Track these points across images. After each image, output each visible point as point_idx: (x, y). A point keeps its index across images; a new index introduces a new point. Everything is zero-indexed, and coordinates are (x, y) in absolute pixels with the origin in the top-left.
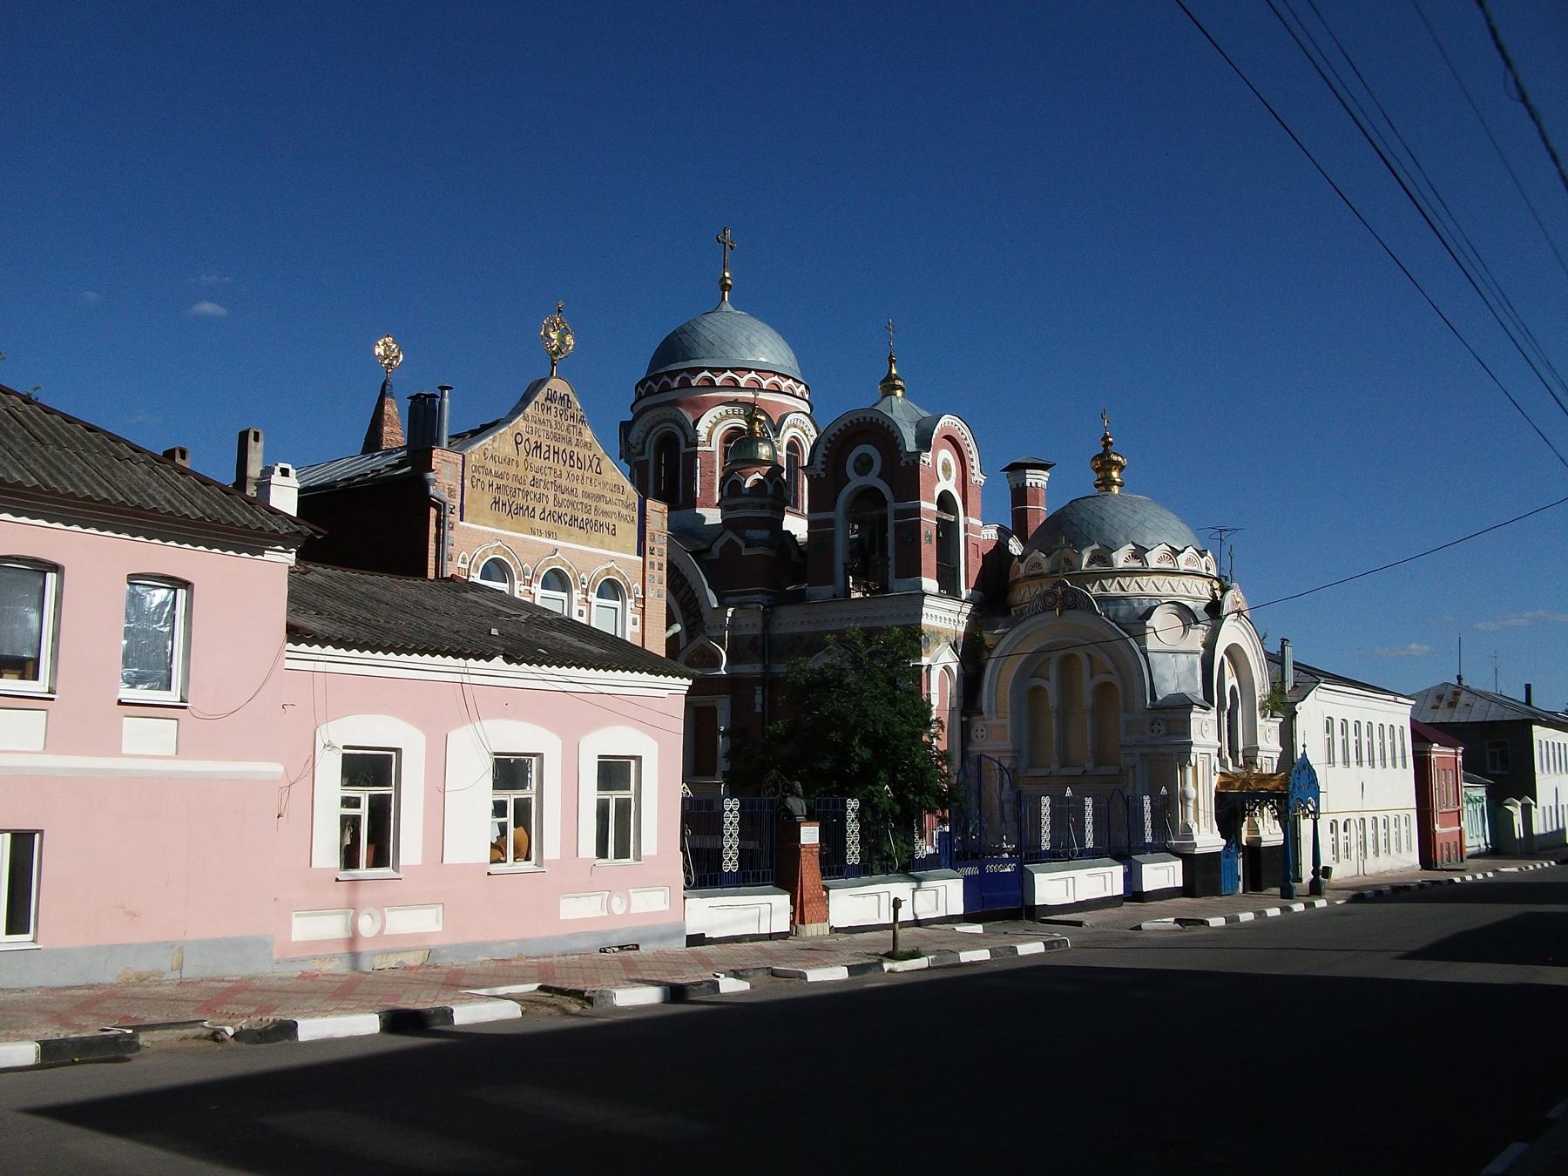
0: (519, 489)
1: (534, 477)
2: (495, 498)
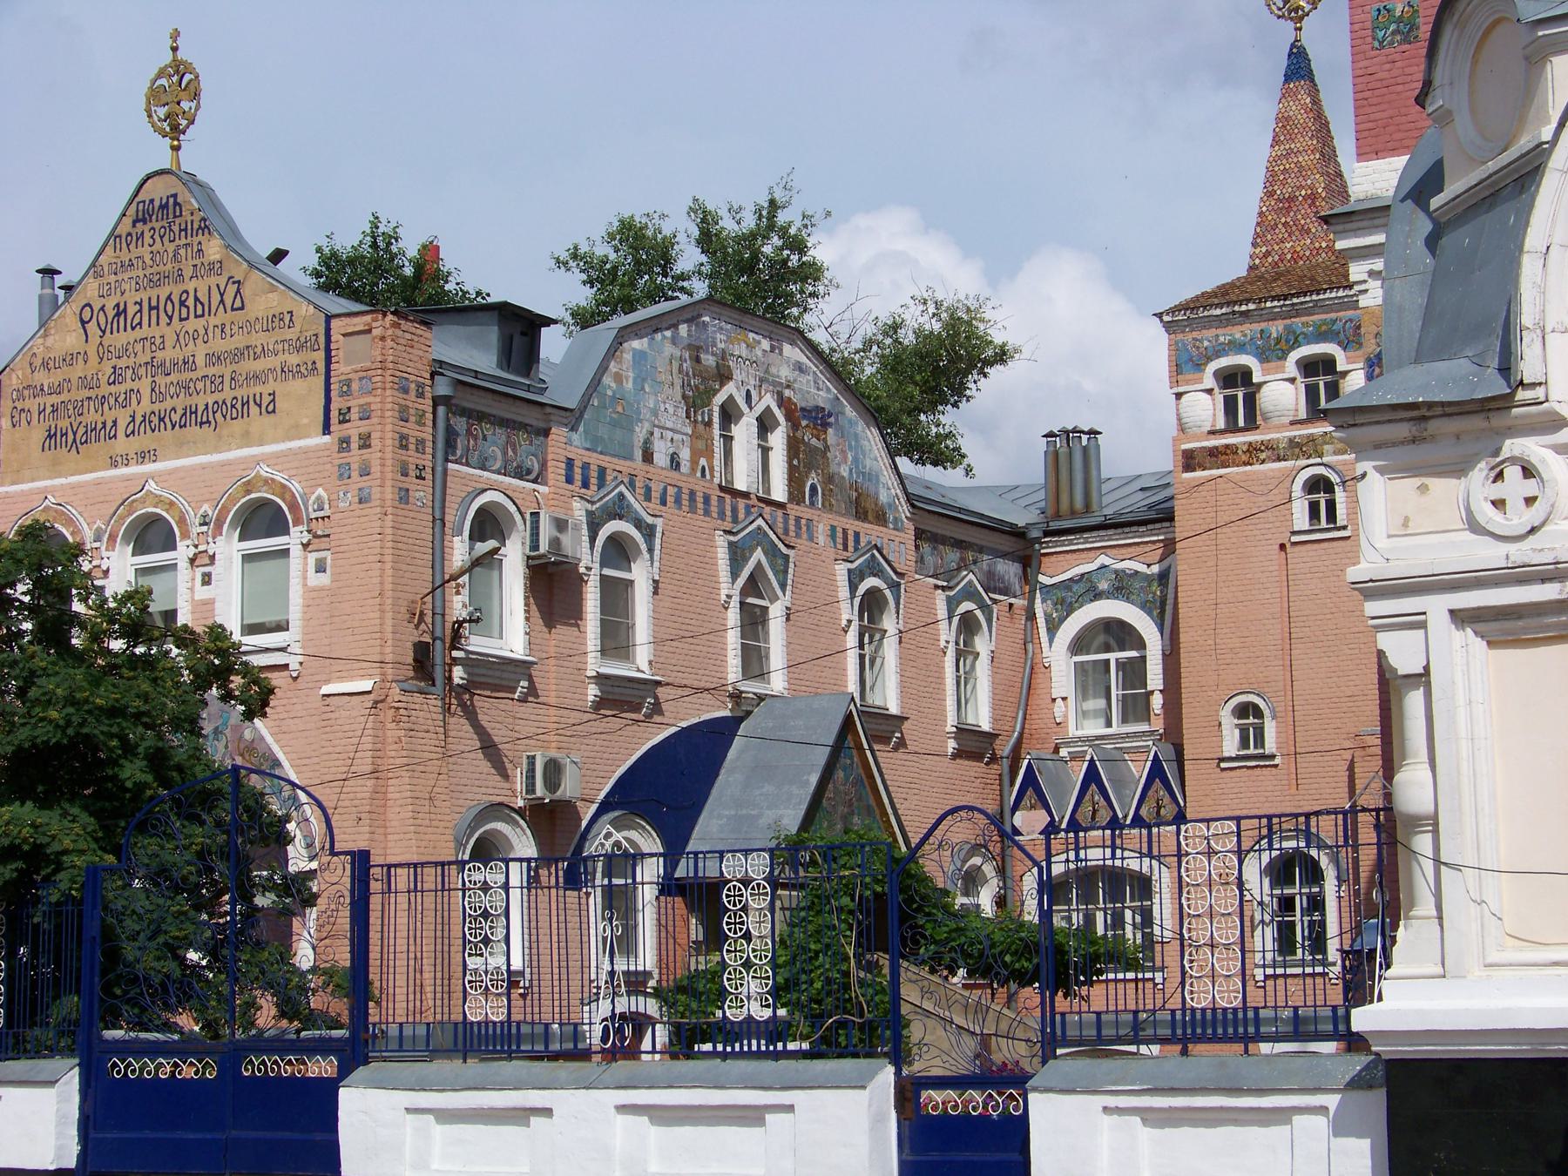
0: (89, 398)
1: (114, 368)
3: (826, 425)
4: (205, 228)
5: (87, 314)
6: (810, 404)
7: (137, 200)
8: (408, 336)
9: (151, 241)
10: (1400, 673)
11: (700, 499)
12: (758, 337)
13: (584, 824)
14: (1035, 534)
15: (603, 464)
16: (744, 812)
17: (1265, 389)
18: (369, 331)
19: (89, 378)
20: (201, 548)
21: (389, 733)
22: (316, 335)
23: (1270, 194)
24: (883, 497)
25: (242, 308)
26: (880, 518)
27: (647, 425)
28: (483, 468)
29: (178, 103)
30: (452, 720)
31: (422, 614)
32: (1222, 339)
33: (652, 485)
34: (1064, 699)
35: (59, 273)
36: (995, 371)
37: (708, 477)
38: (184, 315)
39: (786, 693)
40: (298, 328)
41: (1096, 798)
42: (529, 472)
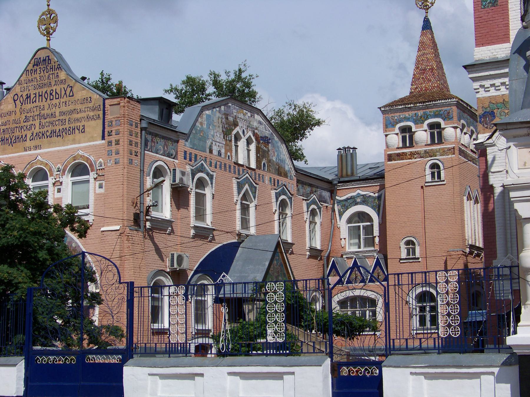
0: (17, 127)
1: (26, 116)
2: (2, 138)
3: (268, 143)
4: (59, 68)
5: (16, 98)
6: (264, 135)
7: (35, 58)
8: (133, 106)
9: (40, 72)
10: (523, 217)
11: (228, 167)
12: (247, 112)
13: (189, 278)
14: (335, 182)
15: (197, 153)
16: (243, 275)
17: (416, 133)
18: (119, 104)
19: (16, 120)
20: (57, 180)
21: (125, 245)
22: (100, 105)
23: (417, 68)
24: (287, 168)
25: (73, 96)
26: (286, 175)
27: (211, 140)
28: (157, 153)
29: (50, 24)
30: (146, 241)
31: (136, 203)
32: (401, 116)
33: (212, 161)
34: (345, 239)
35: (5, 84)
36: (316, 128)
37: (230, 159)
38: (52, 98)
39: (255, 234)
40: (93, 103)
41: (357, 272)
42: (172, 155)
